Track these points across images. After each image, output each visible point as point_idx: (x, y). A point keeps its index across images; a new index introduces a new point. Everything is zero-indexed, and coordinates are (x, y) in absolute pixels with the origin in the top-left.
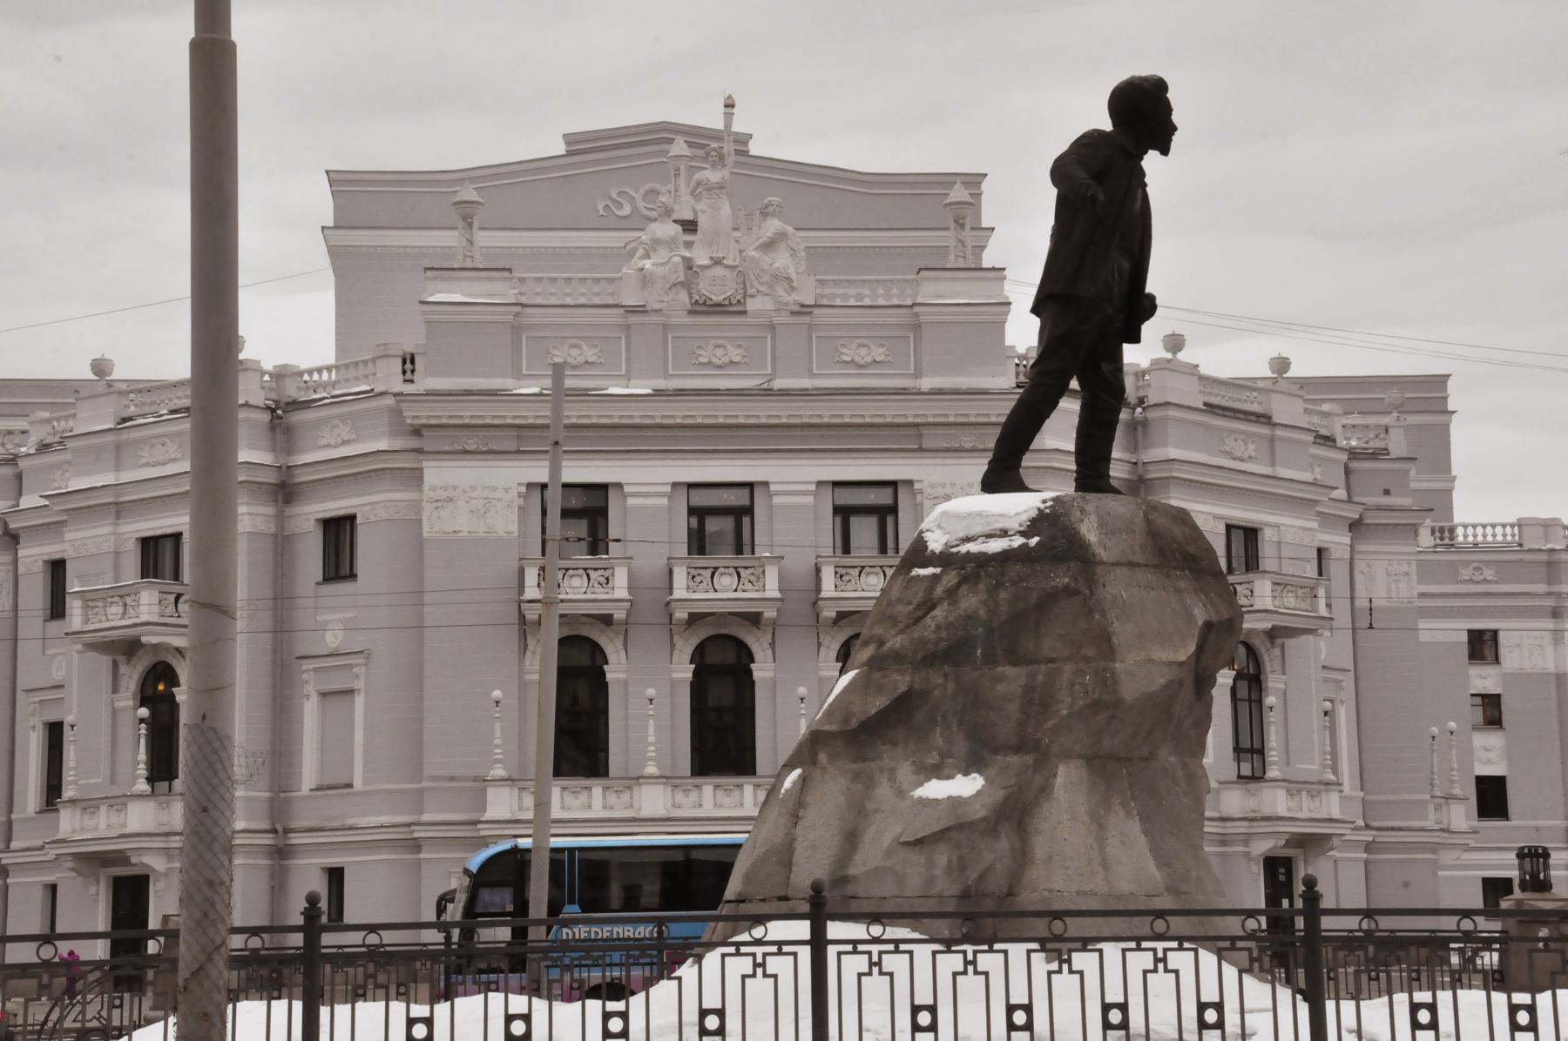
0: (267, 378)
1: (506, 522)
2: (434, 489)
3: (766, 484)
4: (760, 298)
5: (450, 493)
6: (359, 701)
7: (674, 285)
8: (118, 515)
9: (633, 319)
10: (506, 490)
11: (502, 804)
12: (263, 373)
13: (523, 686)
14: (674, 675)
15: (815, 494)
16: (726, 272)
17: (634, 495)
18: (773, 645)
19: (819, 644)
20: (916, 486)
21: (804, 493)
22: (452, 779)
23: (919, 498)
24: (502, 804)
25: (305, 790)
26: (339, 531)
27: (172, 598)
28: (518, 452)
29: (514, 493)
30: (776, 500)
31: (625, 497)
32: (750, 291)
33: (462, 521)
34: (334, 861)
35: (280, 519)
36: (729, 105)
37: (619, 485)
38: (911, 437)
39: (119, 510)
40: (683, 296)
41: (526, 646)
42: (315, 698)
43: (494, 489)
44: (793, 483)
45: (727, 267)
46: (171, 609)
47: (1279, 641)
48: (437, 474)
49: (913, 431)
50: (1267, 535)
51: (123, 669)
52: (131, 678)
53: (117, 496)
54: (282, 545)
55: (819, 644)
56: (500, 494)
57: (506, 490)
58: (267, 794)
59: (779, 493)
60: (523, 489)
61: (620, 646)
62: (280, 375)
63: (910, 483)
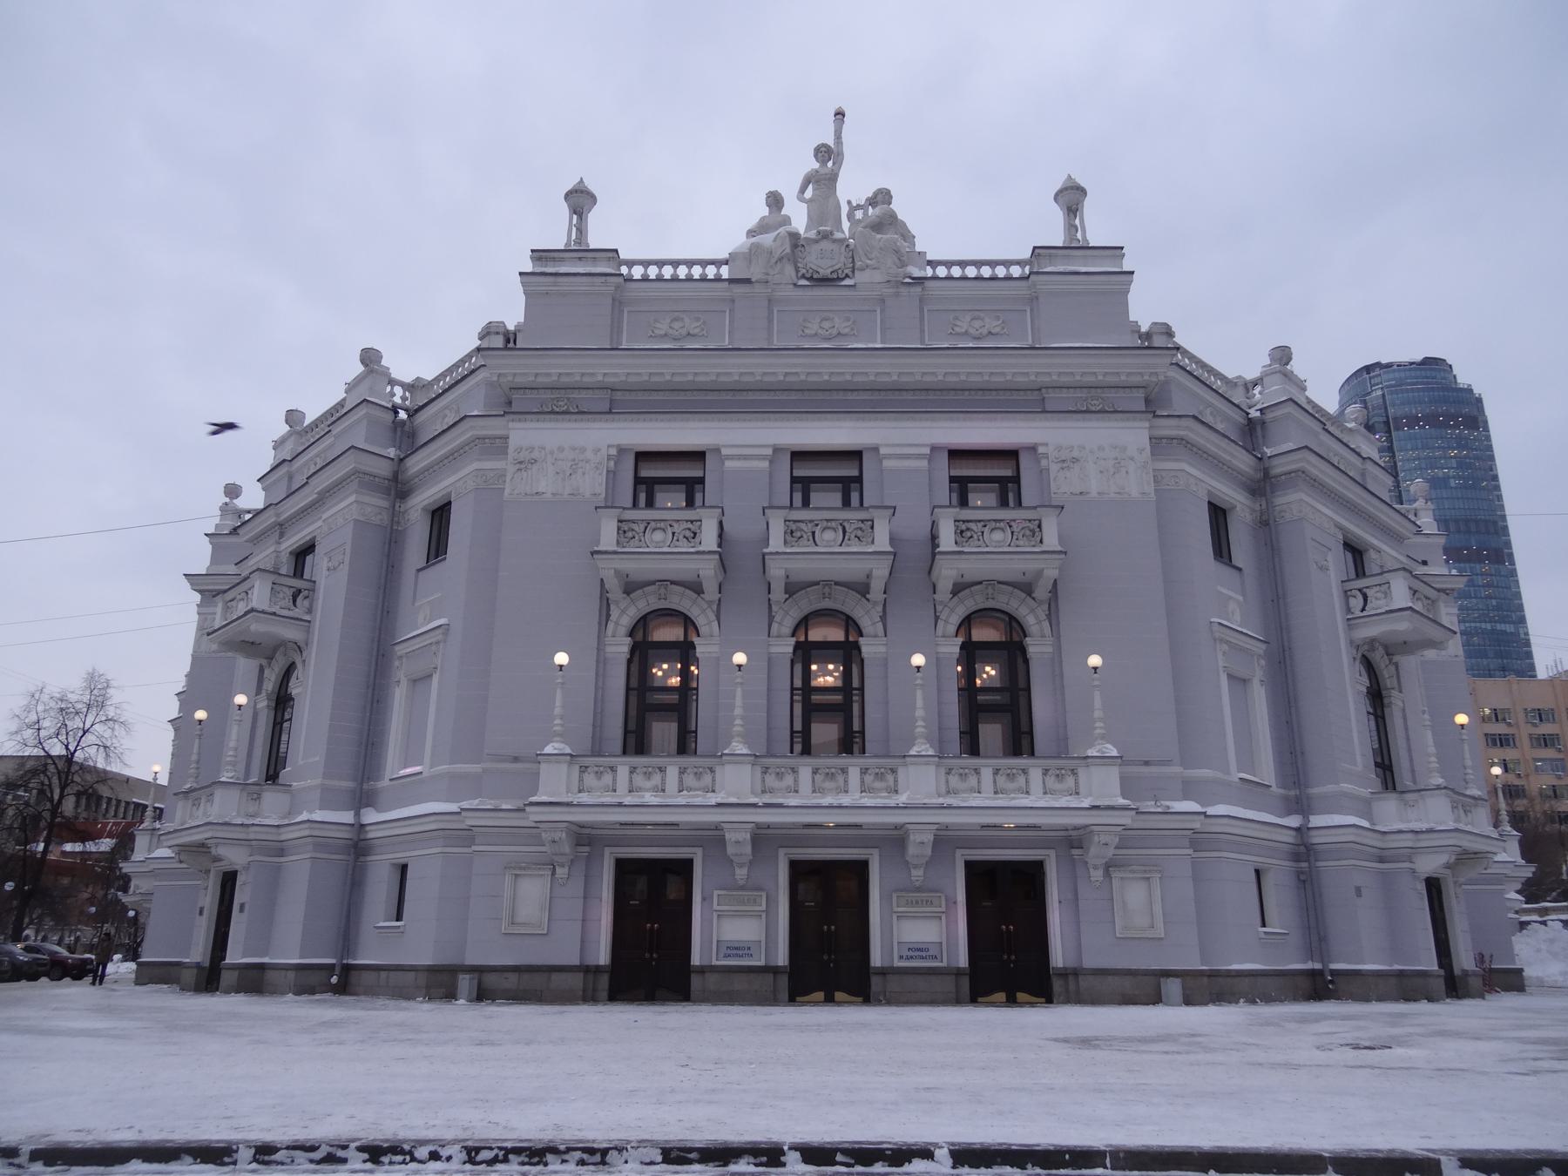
0: (398, 391)
1: (592, 484)
2: (519, 450)
3: (876, 449)
6: (435, 679)
7: (781, 259)
8: (282, 535)
9: (739, 290)
11: (555, 783)
12: (393, 382)
13: (602, 661)
14: (773, 650)
15: (930, 459)
16: (834, 246)
17: (731, 457)
18: (883, 618)
19: (937, 618)
20: (1041, 450)
21: (919, 457)
22: (516, 759)
23: (1044, 463)
24: (555, 783)
25: (385, 783)
26: (440, 515)
27: (289, 592)
28: (610, 412)
29: (604, 452)
30: (887, 463)
31: (722, 459)
32: (858, 264)
33: (545, 482)
34: (400, 856)
36: (840, 114)
37: (717, 450)
38: (1031, 400)
40: (789, 270)
41: (608, 616)
43: (583, 450)
44: (904, 445)
45: (835, 241)
46: (288, 602)
47: (1396, 658)
48: (523, 435)
49: (1035, 396)
50: (1372, 554)
51: (267, 672)
53: (278, 515)
54: (392, 540)
55: (937, 618)
56: (589, 455)
58: (350, 784)
60: (613, 452)
61: (712, 617)
62: (410, 387)
63: (1033, 449)
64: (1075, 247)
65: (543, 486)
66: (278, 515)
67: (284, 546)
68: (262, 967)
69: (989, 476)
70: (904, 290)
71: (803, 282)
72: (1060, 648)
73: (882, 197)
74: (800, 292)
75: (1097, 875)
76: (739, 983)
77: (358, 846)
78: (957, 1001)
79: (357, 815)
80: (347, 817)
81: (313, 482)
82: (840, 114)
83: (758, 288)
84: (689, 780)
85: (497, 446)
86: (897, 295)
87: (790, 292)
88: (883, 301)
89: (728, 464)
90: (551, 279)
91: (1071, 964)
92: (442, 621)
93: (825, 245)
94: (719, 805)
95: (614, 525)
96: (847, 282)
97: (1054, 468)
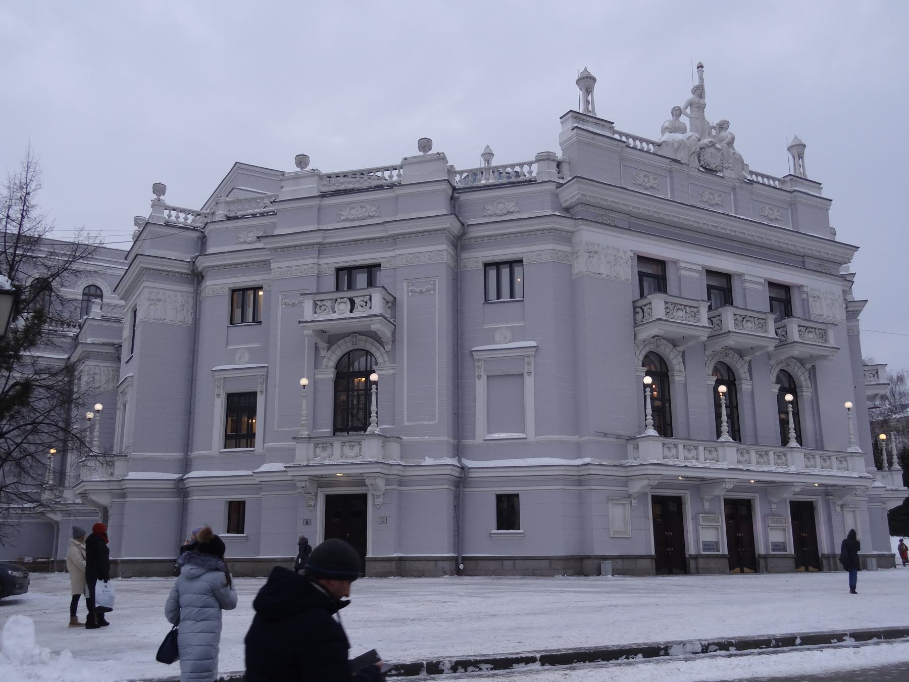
4: (729, 171)
5: (595, 248)
9: (676, 166)
10: (625, 252)
18: (750, 370)
21: (760, 283)
22: (605, 435)
35: (457, 259)
39: (321, 248)
42: (484, 377)
43: (618, 250)
45: (716, 148)
48: (589, 235)
49: (800, 259)
52: (330, 360)
53: (324, 238)
56: (621, 254)
57: (625, 252)
59: (749, 281)
64: (798, 178)
65: (603, 269)
66: (324, 238)
67: (323, 261)
68: (400, 559)
69: (782, 299)
70: (744, 185)
71: (701, 169)
72: (817, 395)
73: (723, 126)
74: (699, 174)
75: (838, 509)
76: (712, 564)
77: (461, 481)
78: (722, 572)
79: (459, 461)
80: (454, 461)
81: (389, 226)
82: (700, 66)
83: (684, 168)
84: (708, 455)
85: (567, 238)
86: (741, 188)
87: (695, 173)
88: (734, 189)
89: (683, 272)
90: (591, 135)
91: (830, 552)
92: (533, 344)
93: (712, 150)
94: (729, 469)
95: (663, 305)
96: (719, 174)
97: (811, 300)
